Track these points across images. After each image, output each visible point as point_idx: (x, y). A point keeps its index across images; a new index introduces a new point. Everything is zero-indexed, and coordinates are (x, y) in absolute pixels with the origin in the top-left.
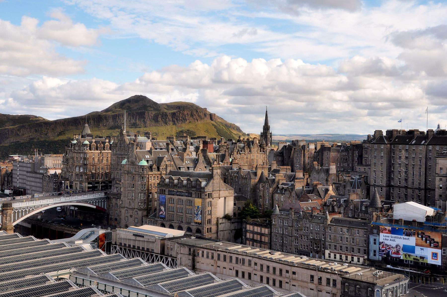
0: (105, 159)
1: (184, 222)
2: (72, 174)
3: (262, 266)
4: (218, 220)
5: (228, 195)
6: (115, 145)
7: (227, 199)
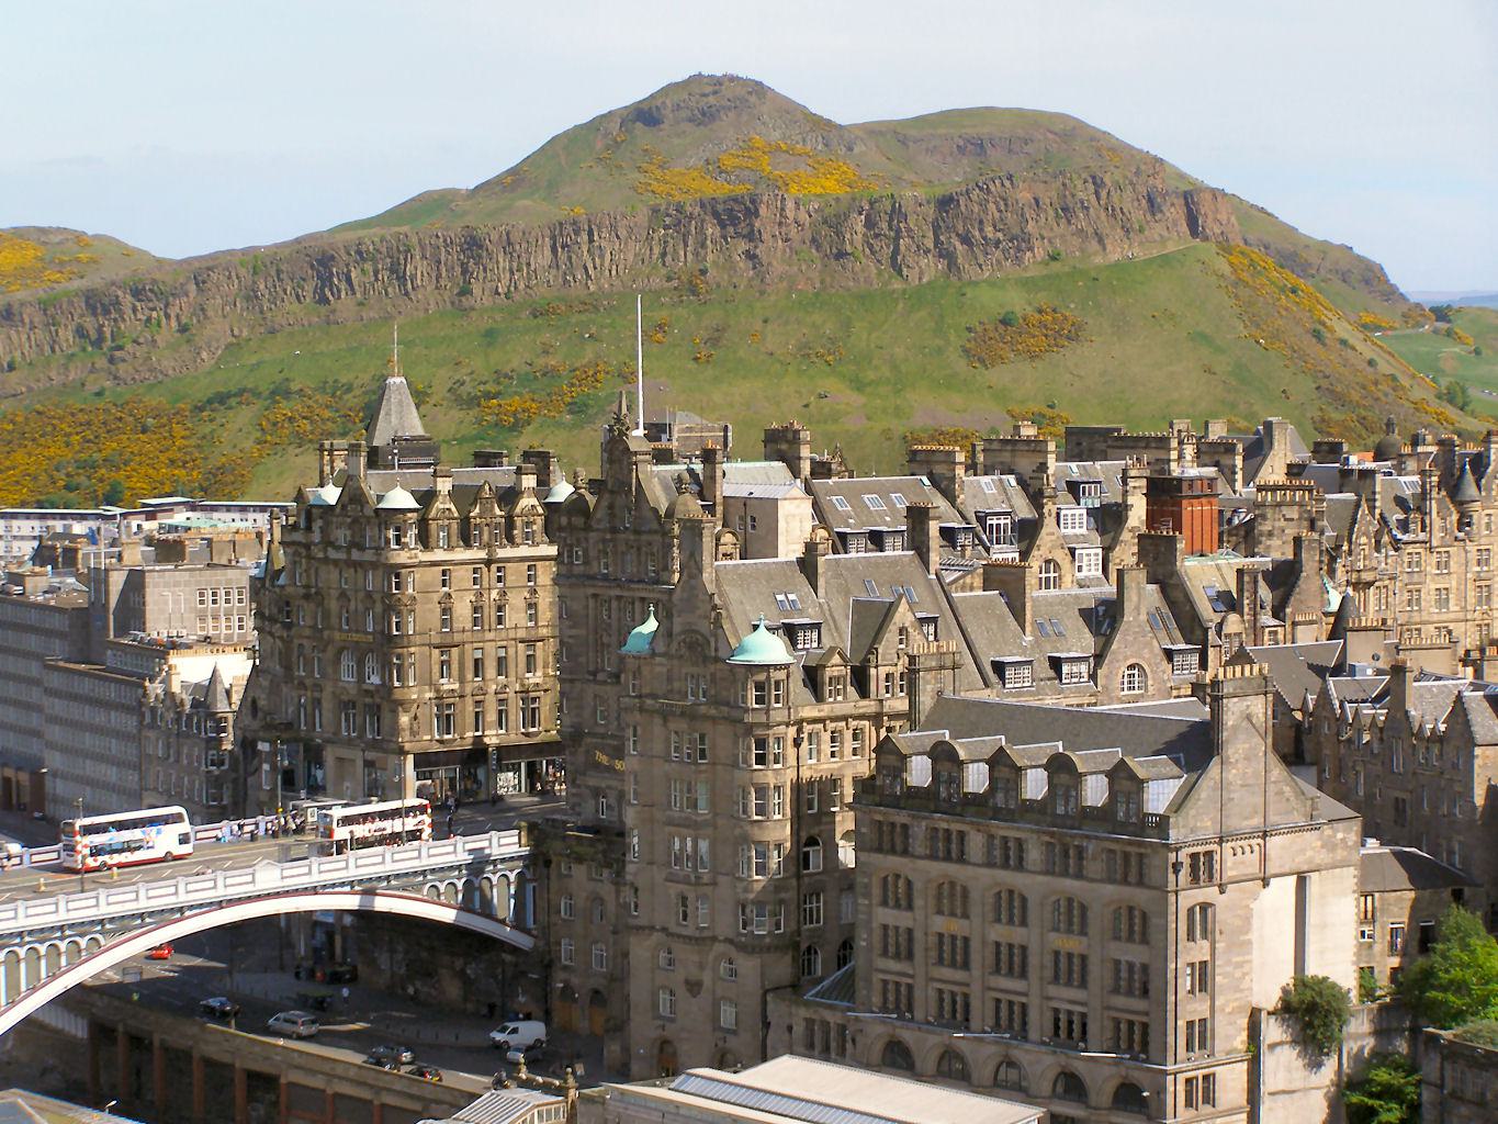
0: (517, 600)
1: (1033, 1034)
2: (317, 702)
5: (1323, 857)
7: (1315, 883)
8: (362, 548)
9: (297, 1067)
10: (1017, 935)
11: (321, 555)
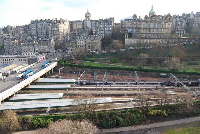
3: (3, 59)
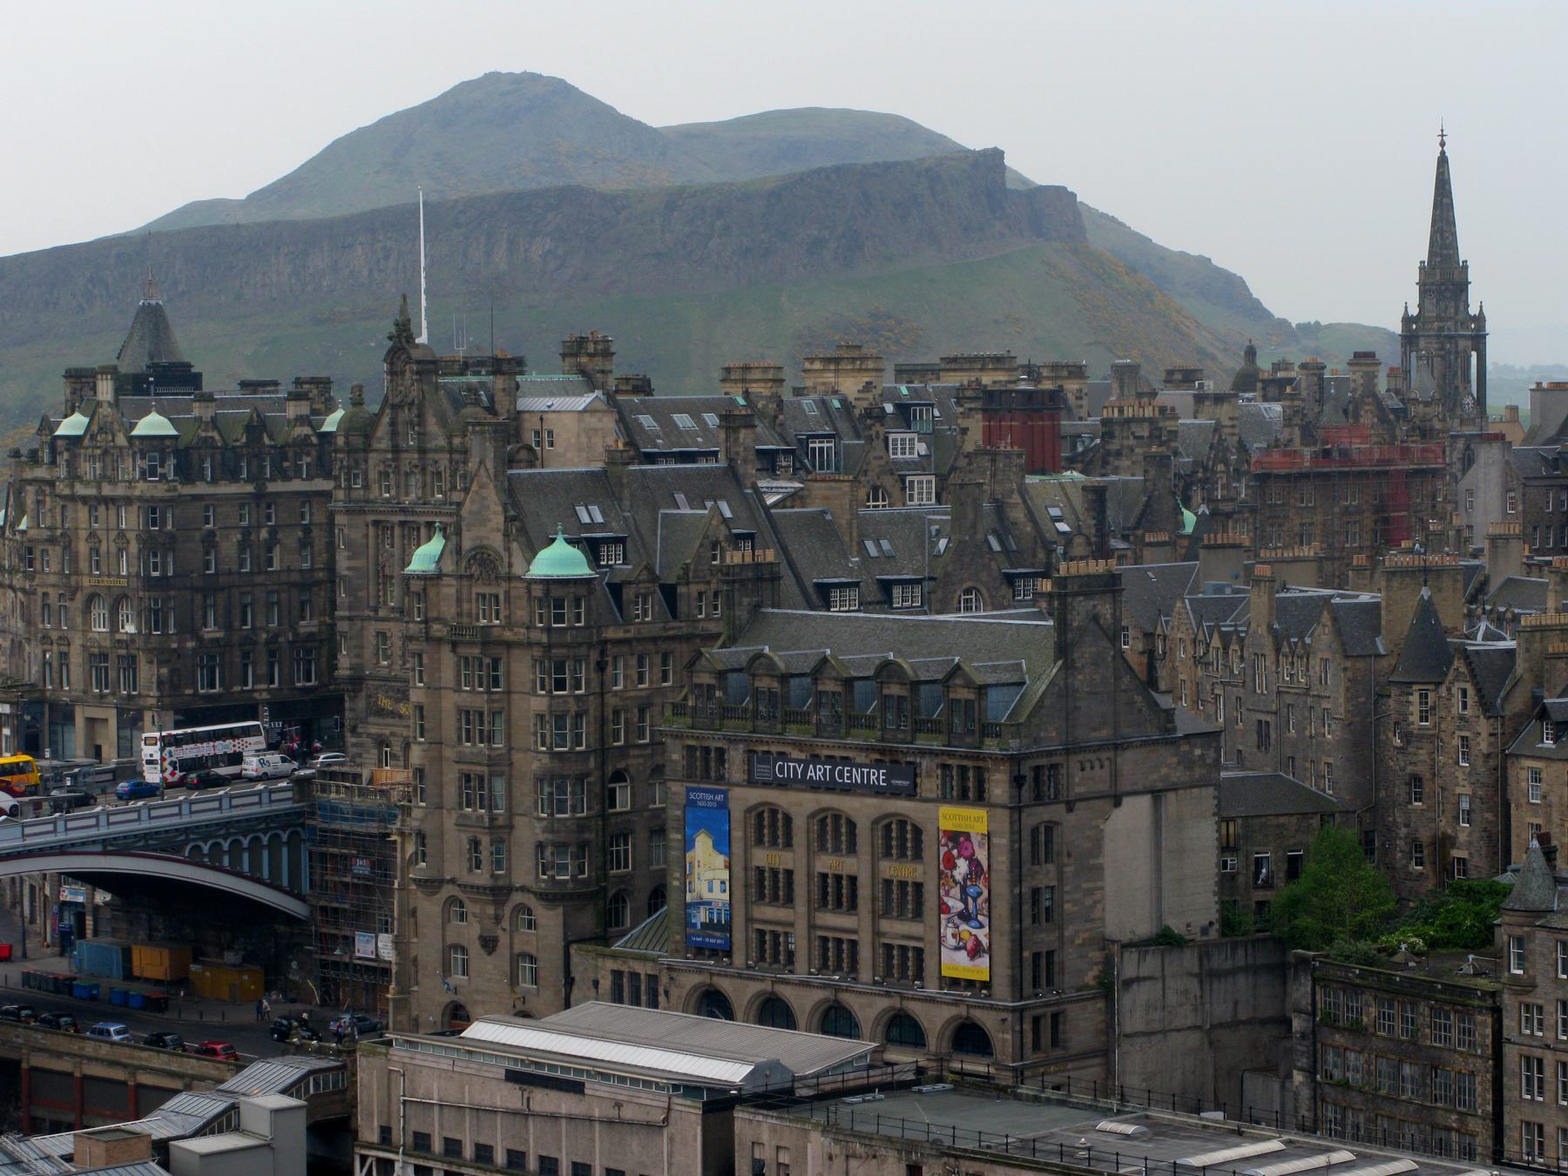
2: (64, 656)
4: (1108, 964)
5: (1178, 775)
6: (358, 441)
8: (113, 481)
9: (40, 1050)
10: (849, 865)
11: (67, 492)
